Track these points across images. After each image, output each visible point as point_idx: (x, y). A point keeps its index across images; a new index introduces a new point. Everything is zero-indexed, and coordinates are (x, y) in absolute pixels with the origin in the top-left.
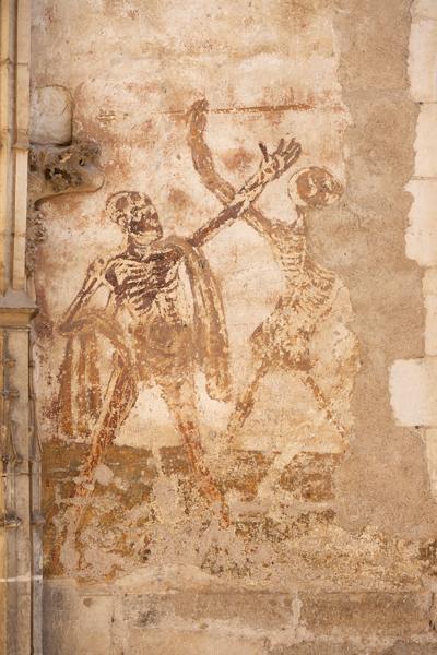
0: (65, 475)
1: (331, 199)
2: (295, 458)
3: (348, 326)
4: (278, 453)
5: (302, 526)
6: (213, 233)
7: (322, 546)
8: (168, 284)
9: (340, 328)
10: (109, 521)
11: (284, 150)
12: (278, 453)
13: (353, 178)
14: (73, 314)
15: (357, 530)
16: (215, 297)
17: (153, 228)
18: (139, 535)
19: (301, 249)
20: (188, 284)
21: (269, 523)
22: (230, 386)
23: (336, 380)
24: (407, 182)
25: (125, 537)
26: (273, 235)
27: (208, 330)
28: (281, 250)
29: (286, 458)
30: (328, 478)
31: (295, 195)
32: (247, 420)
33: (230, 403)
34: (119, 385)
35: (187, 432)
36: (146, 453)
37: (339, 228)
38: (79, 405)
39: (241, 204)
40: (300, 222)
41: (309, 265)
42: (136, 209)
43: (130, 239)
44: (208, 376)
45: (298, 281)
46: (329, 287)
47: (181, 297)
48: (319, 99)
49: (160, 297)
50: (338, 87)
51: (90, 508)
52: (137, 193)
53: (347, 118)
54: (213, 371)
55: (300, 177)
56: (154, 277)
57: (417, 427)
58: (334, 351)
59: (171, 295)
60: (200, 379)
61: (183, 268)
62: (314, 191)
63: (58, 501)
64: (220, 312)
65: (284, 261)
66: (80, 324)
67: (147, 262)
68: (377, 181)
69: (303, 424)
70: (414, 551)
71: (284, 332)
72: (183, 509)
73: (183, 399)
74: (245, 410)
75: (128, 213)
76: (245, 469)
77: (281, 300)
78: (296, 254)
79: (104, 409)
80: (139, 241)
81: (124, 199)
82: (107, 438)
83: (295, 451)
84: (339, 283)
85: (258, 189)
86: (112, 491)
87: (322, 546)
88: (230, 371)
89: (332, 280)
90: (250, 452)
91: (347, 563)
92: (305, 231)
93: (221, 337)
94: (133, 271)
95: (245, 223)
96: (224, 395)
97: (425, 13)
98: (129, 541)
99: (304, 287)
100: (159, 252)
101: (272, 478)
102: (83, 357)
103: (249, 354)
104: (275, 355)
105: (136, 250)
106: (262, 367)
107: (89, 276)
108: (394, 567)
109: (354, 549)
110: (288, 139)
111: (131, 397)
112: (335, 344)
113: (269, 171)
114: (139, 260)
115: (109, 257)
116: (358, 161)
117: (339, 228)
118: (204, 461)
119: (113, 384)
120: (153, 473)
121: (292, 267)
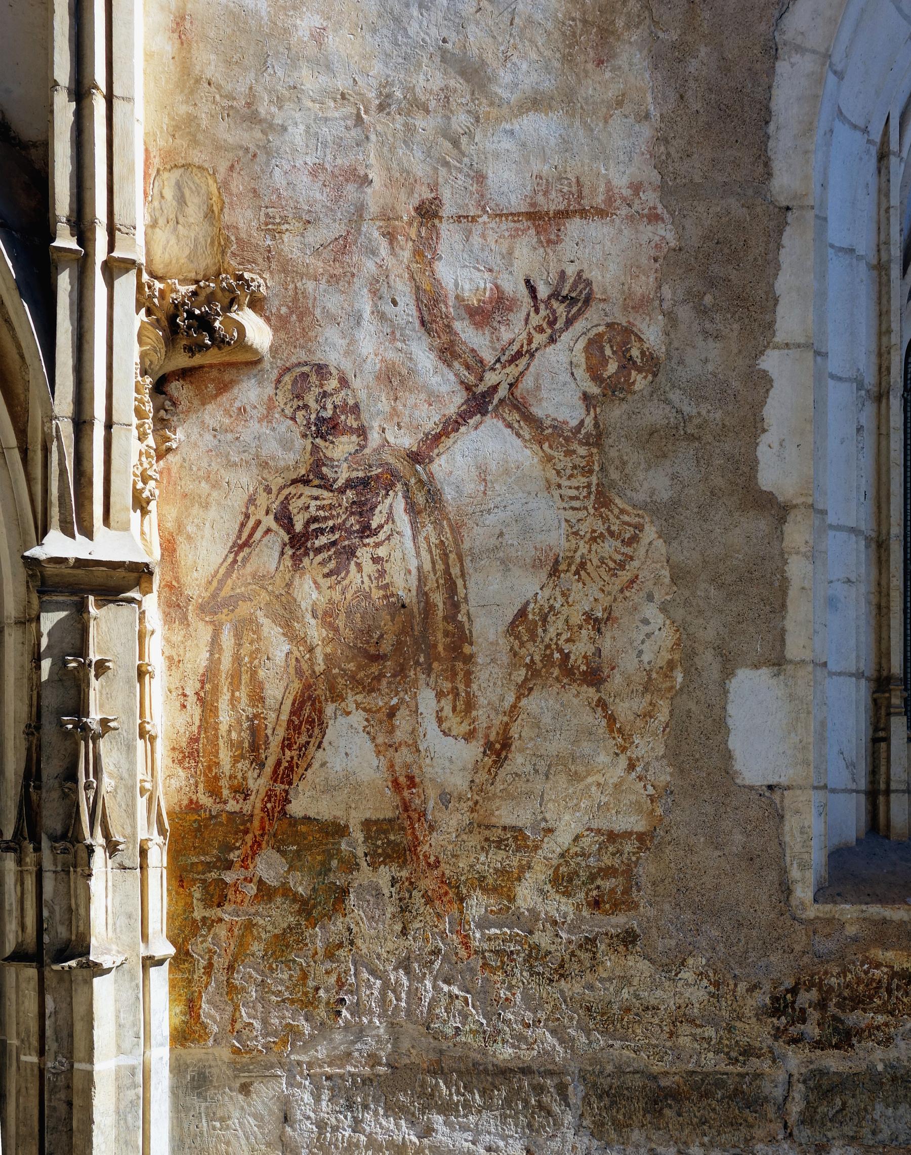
0: (209, 867)
1: (640, 381)
2: (577, 838)
3: (663, 609)
4: (550, 831)
5: (584, 956)
6: (451, 441)
7: (618, 992)
8: (375, 533)
9: (651, 611)
10: (283, 944)
11: (564, 293)
12: (550, 831)
13: (676, 344)
14: (222, 583)
15: (669, 966)
16: (452, 556)
17: (351, 431)
18: (328, 973)
19: (591, 472)
20: (408, 532)
21: (534, 954)
22: (474, 713)
23: (640, 704)
24: (762, 353)
25: (305, 976)
26: (546, 446)
27: (440, 614)
28: (558, 473)
29: (563, 839)
30: (628, 873)
31: (580, 373)
32: (502, 773)
33: (474, 743)
34: (296, 711)
35: (406, 793)
36: (338, 830)
37: (651, 434)
38: (232, 745)
39: (495, 388)
40: (589, 421)
41: (603, 500)
42: (325, 395)
43: (315, 448)
44: (440, 695)
45: (584, 528)
46: (634, 539)
47: (398, 554)
48: (624, 199)
49: (364, 555)
50: (655, 177)
51: (249, 926)
52: (326, 366)
53: (666, 232)
54: (447, 686)
55: (591, 342)
56: (352, 520)
57: (770, 787)
58: (641, 652)
59: (382, 552)
60: (427, 700)
61: (400, 505)
62: (612, 367)
63: (198, 913)
64: (459, 582)
65: (563, 492)
66: (231, 603)
67: (342, 490)
68: (713, 350)
69: (590, 780)
70: (763, 998)
71: (562, 618)
72: (398, 927)
73: (399, 735)
74: (498, 755)
75: (313, 405)
76: (496, 858)
77: (557, 562)
78: (582, 481)
79: (272, 754)
80: (329, 454)
81: (305, 376)
82: (277, 803)
83: (576, 828)
84: (650, 533)
85: (523, 362)
86: (285, 895)
87: (618, 992)
88: (475, 686)
89: (639, 527)
90: (504, 828)
91: (656, 1020)
92: (597, 439)
93: (460, 626)
94: (320, 508)
95: (500, 424)
96: (465, 728)
97: (799, 40)
98: (311, 984)
99: (594, 539)
100: (361, 474)
101: (538, 874)
102: (237, 659)
103: (505, 658)
104: (547, 659)
105: (324, 469)
106: (526, 680)
107: (247, 516)
108: (730, 1029)
109: (665, 997)
110: (571, 270)
111: (317, 730)
112: (644, 639)
113: (540, 329)
114: (328, 487)
115: (280, 481)
116: (685, 313)
117: (651, 434)
118: (434, 844)
119: (287, 708)
120: (351, 866)
121: (576, 504)
